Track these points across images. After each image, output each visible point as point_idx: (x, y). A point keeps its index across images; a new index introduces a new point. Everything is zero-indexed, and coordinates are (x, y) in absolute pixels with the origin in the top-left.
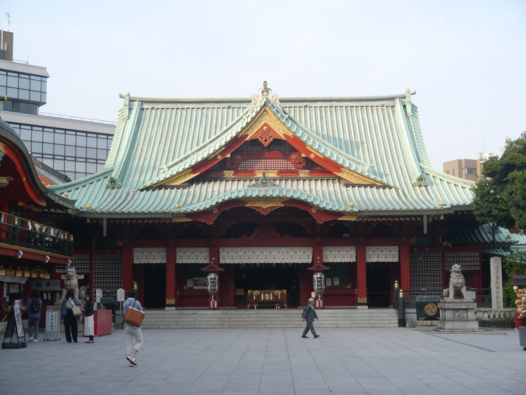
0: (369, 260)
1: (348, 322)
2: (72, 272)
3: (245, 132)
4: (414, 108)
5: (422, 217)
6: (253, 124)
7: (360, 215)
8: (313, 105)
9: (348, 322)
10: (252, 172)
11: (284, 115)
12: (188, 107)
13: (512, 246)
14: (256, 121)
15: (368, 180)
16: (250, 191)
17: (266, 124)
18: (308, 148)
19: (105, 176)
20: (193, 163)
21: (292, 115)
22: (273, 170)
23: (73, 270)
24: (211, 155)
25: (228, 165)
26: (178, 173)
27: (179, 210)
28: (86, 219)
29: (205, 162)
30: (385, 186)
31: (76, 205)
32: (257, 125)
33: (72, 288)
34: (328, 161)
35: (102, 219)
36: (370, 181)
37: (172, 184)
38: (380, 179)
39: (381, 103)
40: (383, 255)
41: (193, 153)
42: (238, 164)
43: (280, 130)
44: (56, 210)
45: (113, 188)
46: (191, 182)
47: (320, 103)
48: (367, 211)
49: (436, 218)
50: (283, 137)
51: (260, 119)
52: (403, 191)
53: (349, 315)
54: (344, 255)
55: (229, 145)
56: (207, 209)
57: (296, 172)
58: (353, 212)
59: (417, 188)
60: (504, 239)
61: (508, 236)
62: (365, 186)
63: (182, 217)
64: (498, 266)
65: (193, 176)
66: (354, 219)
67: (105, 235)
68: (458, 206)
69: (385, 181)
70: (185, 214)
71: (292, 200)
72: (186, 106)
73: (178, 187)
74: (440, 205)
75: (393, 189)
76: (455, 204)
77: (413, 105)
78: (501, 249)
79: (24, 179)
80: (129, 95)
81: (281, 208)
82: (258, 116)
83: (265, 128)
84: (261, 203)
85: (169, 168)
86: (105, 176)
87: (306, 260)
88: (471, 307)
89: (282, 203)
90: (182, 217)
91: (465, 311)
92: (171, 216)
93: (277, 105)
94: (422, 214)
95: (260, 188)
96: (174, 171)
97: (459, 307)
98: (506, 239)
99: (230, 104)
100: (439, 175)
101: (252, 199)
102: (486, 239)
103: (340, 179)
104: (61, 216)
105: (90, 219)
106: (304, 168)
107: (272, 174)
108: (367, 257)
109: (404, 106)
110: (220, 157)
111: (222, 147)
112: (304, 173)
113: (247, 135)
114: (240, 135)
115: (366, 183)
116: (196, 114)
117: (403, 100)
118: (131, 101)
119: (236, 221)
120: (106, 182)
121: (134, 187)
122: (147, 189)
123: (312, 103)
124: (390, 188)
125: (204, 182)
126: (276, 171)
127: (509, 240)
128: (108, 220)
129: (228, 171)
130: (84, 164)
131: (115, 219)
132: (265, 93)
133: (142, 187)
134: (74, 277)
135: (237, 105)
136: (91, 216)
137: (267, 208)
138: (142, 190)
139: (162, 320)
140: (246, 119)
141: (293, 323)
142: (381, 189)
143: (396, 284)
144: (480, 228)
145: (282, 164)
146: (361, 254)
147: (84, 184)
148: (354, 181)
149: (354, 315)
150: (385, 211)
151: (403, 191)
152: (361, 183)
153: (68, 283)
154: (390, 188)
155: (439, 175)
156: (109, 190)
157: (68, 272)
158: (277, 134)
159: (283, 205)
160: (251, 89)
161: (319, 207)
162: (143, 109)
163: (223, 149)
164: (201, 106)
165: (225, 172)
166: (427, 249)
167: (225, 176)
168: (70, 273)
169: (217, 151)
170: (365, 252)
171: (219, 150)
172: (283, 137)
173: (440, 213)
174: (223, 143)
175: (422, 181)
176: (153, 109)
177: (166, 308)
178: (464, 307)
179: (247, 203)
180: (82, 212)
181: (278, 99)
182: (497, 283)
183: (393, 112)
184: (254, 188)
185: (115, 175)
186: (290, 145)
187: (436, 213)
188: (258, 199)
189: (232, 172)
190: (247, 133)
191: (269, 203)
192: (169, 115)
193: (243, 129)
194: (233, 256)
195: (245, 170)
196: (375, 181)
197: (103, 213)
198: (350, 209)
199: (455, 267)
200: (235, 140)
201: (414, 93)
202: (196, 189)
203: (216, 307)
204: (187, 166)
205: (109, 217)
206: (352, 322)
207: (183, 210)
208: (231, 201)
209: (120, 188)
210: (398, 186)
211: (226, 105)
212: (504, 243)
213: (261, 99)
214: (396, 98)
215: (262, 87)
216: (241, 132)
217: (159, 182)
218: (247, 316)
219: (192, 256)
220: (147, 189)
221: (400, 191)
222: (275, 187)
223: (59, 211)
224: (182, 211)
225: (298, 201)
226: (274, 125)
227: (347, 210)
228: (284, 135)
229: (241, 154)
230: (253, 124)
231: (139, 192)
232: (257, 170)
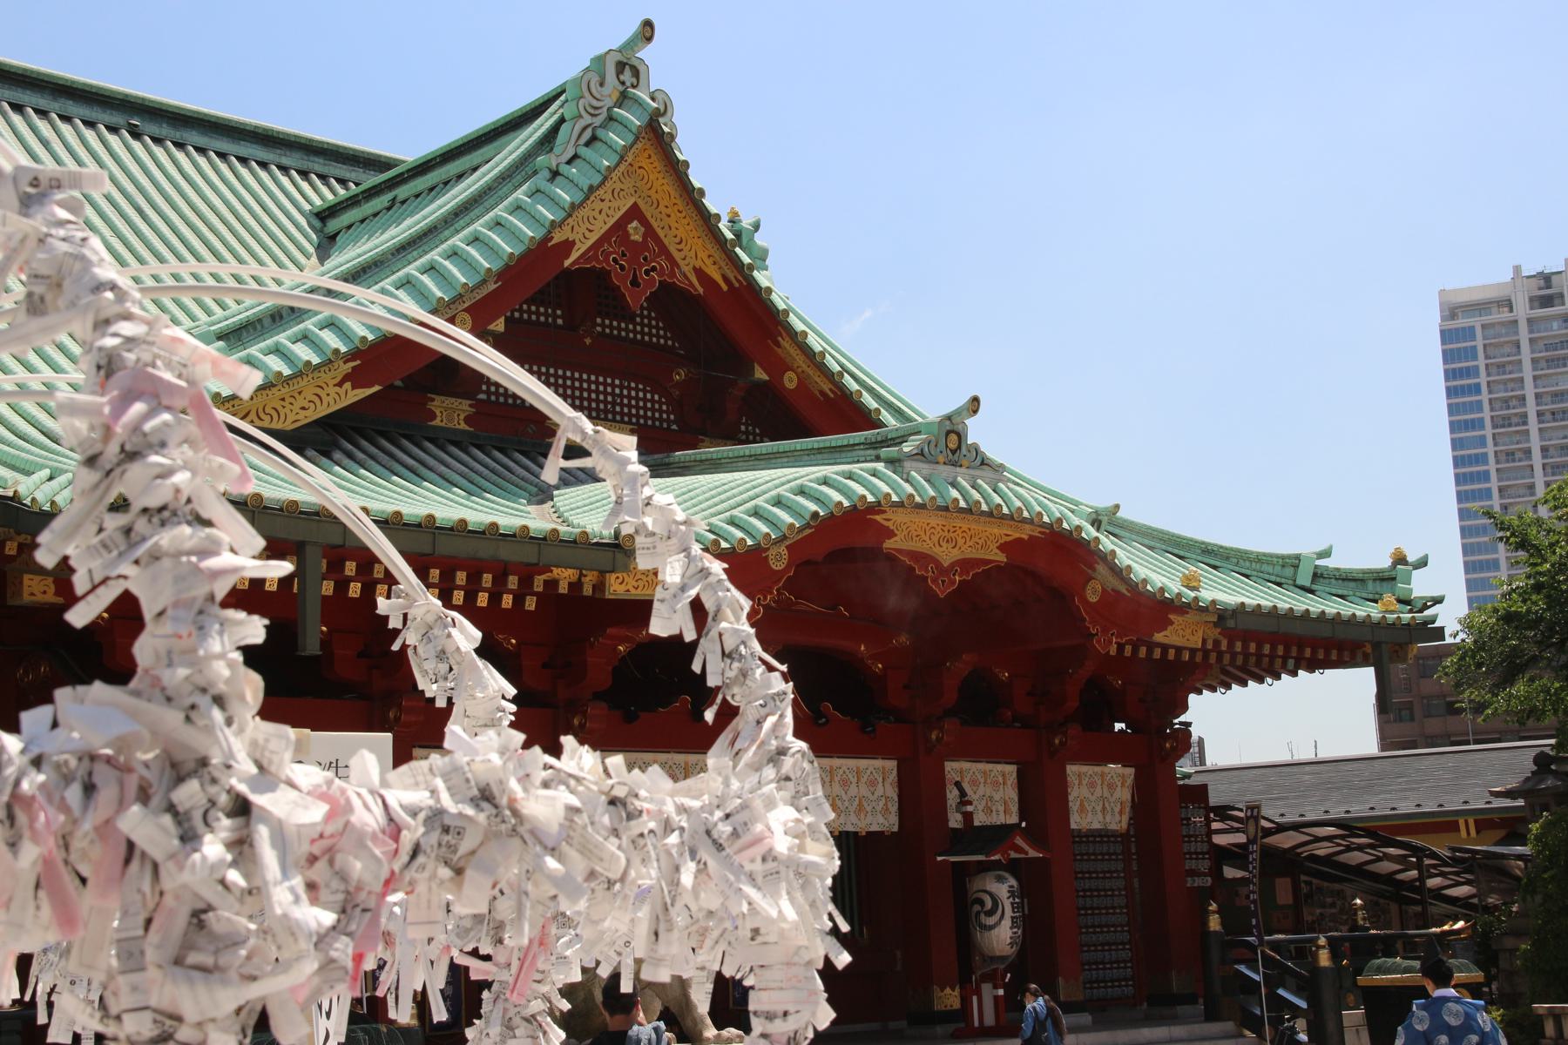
17: (634, 213)
82: (622, 167)
87: (881, 820)
113: (568, 246)
114: (558, 237)
132: (627, 76)
137: (953, 565)
163: (492, 287)
167: (437, 422)
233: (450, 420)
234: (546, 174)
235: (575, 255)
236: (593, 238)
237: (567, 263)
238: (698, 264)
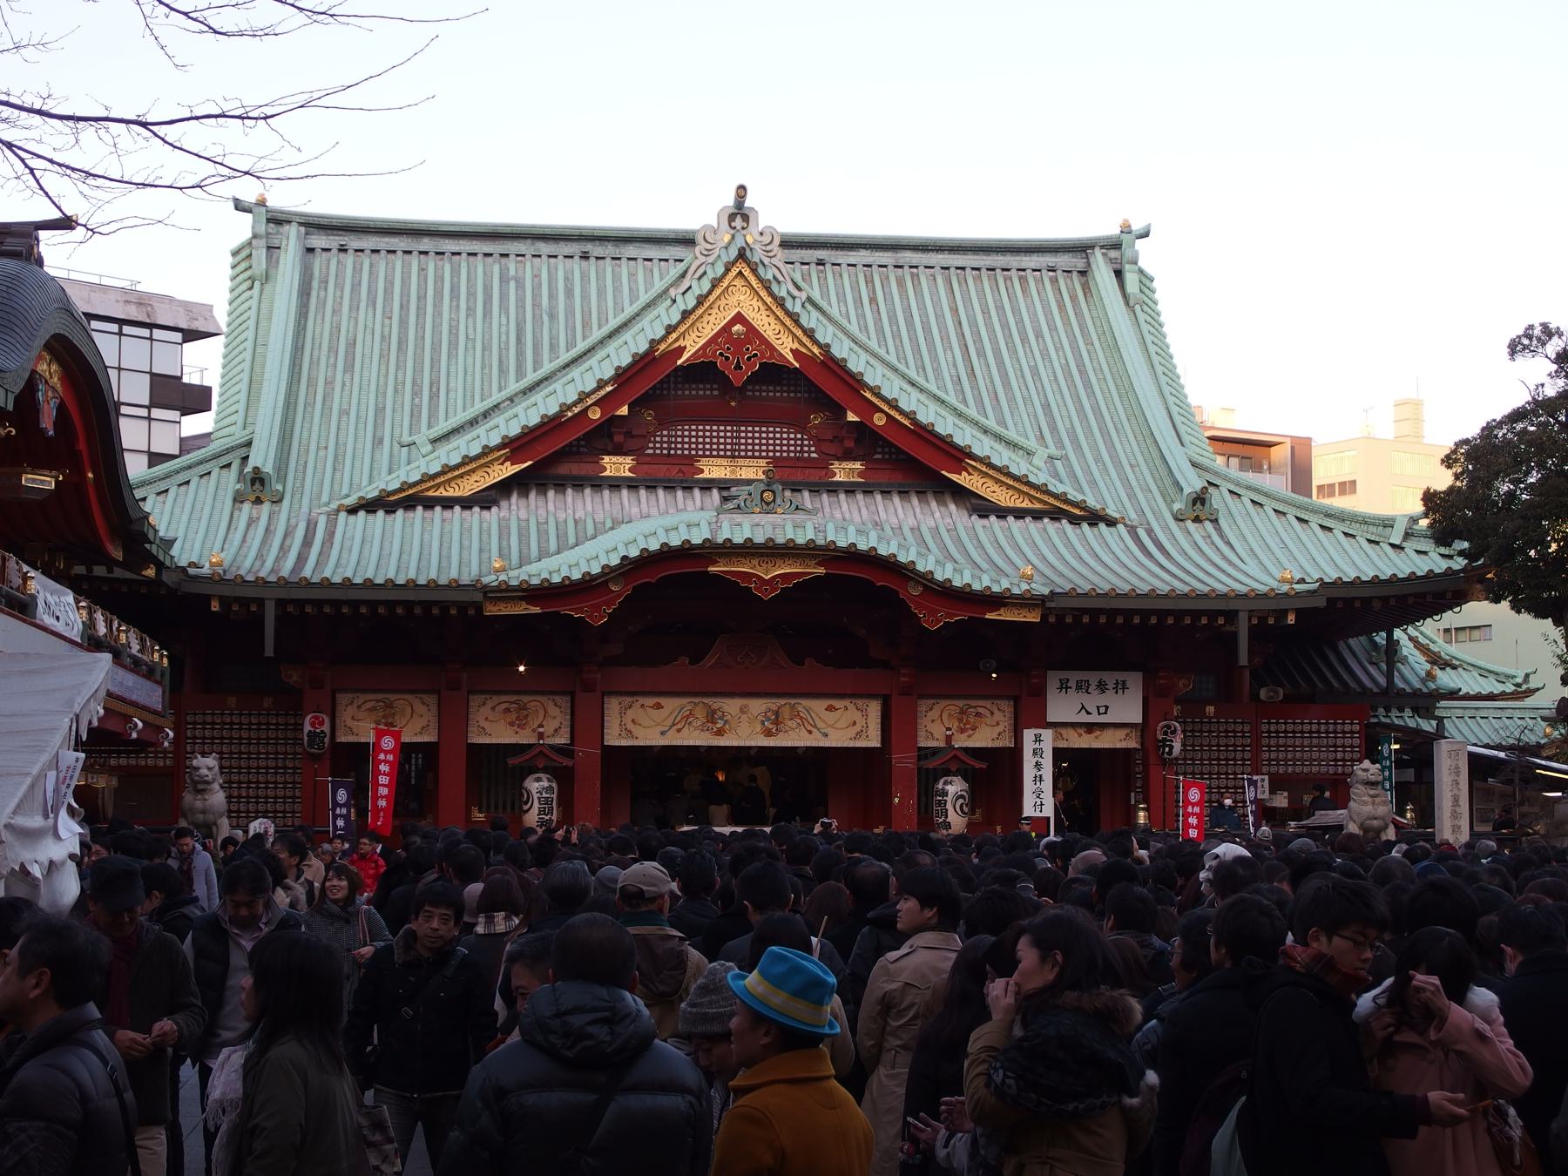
2: (210, 769)
3: (677, 340)
4: (1145, 279)
5: (1231, 616)
6: (701, 316)
7: (1052, 605)
8: (844, 257)
10: (690, 461)
11: (795, 292)
12: (456, 249)
13: (1443, 703)
14: (710, 307)
15: (1045, 498)
16: (726, 525)
17: (739, 319)
18: (868, 395)
19: (224, 460)
20: (514, 430)
21: (816, 295)
22: (753, 457)
23: (211, 761)
24: (569, 408)
25: (618, 438)
26: (467, 460)
27: (503, 577)
28: (207, 599)
29: (551, 426)
30: (1095, 518)
31: (175, 551)
32: (712, 319)
33: (211, 817)
34: (925, 434)
35: (260, 602)
36: (1051, 501)
37: (445, 494)
38: (1080, 497)
39: (1049, 260)
41: (511, 399)
42: (646, 437)
43: (784, 338)
44: (110, 571)
45: (258, 501)
46: (504, 488)
47: (863, 253)
48: (1071, 594)
49: (1271, 621)
50: (790, 357)
51: (723, 302)
52: (1150, 532)
55: (624, 377)
56: (594, 578)
57: (823, 465)
58: (1033, 598)
59: (1189, 523)
60: (1417, 685)
61: (1429, 674)
62: (1037, 516)
63: (513, 598)
64: (1457, 767)
65: (509, 470)
66: (1033, 617)
67: (269, 651)
68: (1338, 583)
69: (1092, 502)
70: (524, 590)
71: (852, 556)
72: (449, 246)
73: (467, 503)
74: (1284, 581)
75: (1120, 527)
76: (1332, 575)
77: (1141, 271)
78: (1408, 712)
79: (90, 475)
80: (262, 203)
81: (818, 578)
82: (718, 292)
83: (737, 328)
84: (755, 562)
85: (434, 441)
86: (224, 460)
89: (819, 564)
90: (513, 598)
92: (479, 597)
93: (774, 261)
94: (1232, 606)
95: (757, 518)
96: (452, 453)
98: (1423, 681)
99: (589, 247)
100: (1249, 488)
101: (730, 550)
102: (1368, 684)
103: (961, 495)
104: (125, 589)
105: (224, 601)
106: (847, 456)
107: (752, 470)
109: (1119, 274)
110: (595, 414)
111: (607, 383)
112: (844, 471)
113: (682, 350)
114: (662, 347)
115: (1038, 506)
116: (481, 271)
117: (1113, 254)
118: (278, 220)
119: (676, 612)
120: (230, 481)
121: (325, 498)
122: (370, 506)
124: (1111, 523)
125: (542, 489)
126: (763, 462)
127: (1432, 686)
128: (281, 603)
129: (615, 459)
130: (146, 423)
131: (300, 603)
132: (738, 222)
133: (351, 501)
134: (216, 786)
135: (610, 250)
136: (227, 591)
138: (352, 511)
140: (679, 299)
142: (1085, 526)
143: (1141, 814)
144: (1342, 645)
145: (786, 441)
147: (162, 486)
148: (1002, 497)
150: (1125, 595)
151: (1150, 532)
152: (1023, 505)
153: (199, 804)
154: (1111, 523)
155: (1249, 488)
156: (247, 506)
157: (197, 769)
158: (772, 349)
159: (822, 571)
160: (696, 209)
161: (933, 580)
162: (311, 250)
163: (609, 388)
164: (495, 247)
165: (607, 459)
166: (1210, 709)
167: (607, 473)
168: (204, 771)
169: (588, 395)
171: (593, 392)
172: (790, 357)
173: (1284, 605)
174: (609, 373)
176: (343, 250)
179: (714, 563)
180: (196, 578)
181: (777, 241)
182: (1455, 815)
183: (1086, 288)
184: (738, 518)
185: (262, 457)
186: (811, 386)
187: (1273, 606)
188: (748, 550)
189: (629, 460)
190: (681, 343)
191: (779, 562)
192: (399, 271)
193: (670, 329)
194: (649, 723)
195: (669, 455)
196: (1067, 501)
197: (261, 583)
198: (1024, 587)
199: (1366, 770)
200: (645, 362)
201: (1145, 235)
202: (516, 509)
204: (495, 440)
205: (283, 594)
207: (515, 577)
208: (667, 555)
209: (280, 501)
210: (1133, 515)
211: (574, 248)
212: (1417, 694)
213: (727, 238)
214: (1092, 247)
215: (730, 201)
216: (664, 338)
217: (405, 486)
220: (370, 506)
221: (1142, 533)
222: (800, 516)
223: (80, 570)
224: (514, 583)
225: (871, 559)
226: (766, 320)
227: (1016, 591)
228: (795, 352)
229: (664, 405)
230: (701, 316)
231: (343, 515)
232: (704, 456)
233: (618, 470)
234: (669, 302)
236: (702, 342)
238: (796, 346)
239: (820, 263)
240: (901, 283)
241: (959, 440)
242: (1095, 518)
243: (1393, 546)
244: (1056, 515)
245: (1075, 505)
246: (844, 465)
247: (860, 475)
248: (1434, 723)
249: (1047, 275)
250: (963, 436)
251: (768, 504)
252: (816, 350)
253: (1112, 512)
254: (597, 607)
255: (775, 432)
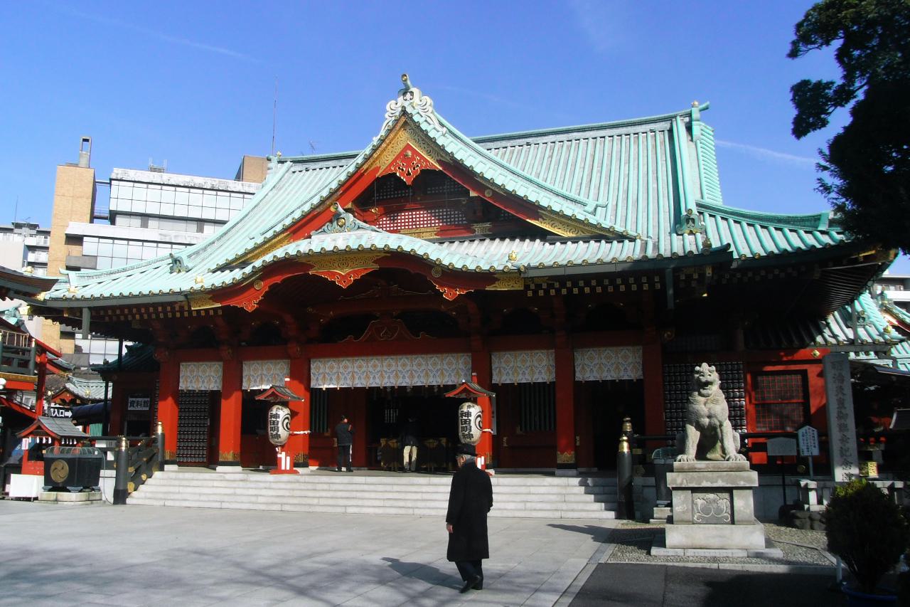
0: (579, 376)
1: (511, 506)
9: (511, 506)
17: (408, 147)
30: (621, 237)
35: (80, 310)
39: (652, 126)
40: (606, 365)
45: (180, 271)
47: (551, 136)
53: (523, 490)
54: (525, 368)
55: (345, 187)
66: (519, 287)
88: (742, 484)
89: (375, 262)
91: (727, 495)
92: (181, 298)
97: (705, 484)
100: (733, 213)
108: (578, 370)
113: (377, 169)
123: (539, 138)
124: (632, 240)
137: (348, 274)
138: (214, 272)
139: (181, 489)
141: (401, 504)
146: (565, 366)
149: (532, 490)
159: (376, 267)
170: (573, 360)
175: (694, 223)
176: (307, 170)
177: (219, 469)
178: (720, 484)
179: (312, 267)
184: (322, 236)
194: (332, 375)
203: (288, 468)
206: (521, 506)
218: (325, 487)
219: (263, 377)
228: (439, 162)
235: (380, 171)
237: (377, 176)
238: (440, 158)
239: (528, 144)
240: (569, 148)
241: (532, 198)
242: (621, 237)
243: (822, 232)
244: (598, 238)
245: (608, 230)
246: (480, 225)
247: (490, 230)
248: (890, 362)
249: (650, 134)
250: (533, 195)
251: (341, 226)
252: (448, 158)
253: (632, 233)
254: (250, 301)
255: (439, 212)
